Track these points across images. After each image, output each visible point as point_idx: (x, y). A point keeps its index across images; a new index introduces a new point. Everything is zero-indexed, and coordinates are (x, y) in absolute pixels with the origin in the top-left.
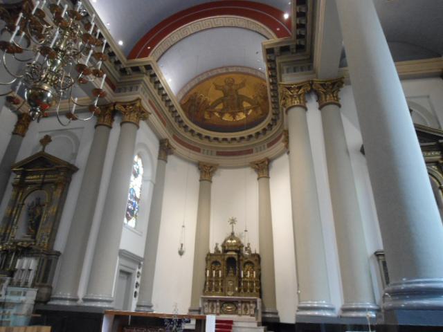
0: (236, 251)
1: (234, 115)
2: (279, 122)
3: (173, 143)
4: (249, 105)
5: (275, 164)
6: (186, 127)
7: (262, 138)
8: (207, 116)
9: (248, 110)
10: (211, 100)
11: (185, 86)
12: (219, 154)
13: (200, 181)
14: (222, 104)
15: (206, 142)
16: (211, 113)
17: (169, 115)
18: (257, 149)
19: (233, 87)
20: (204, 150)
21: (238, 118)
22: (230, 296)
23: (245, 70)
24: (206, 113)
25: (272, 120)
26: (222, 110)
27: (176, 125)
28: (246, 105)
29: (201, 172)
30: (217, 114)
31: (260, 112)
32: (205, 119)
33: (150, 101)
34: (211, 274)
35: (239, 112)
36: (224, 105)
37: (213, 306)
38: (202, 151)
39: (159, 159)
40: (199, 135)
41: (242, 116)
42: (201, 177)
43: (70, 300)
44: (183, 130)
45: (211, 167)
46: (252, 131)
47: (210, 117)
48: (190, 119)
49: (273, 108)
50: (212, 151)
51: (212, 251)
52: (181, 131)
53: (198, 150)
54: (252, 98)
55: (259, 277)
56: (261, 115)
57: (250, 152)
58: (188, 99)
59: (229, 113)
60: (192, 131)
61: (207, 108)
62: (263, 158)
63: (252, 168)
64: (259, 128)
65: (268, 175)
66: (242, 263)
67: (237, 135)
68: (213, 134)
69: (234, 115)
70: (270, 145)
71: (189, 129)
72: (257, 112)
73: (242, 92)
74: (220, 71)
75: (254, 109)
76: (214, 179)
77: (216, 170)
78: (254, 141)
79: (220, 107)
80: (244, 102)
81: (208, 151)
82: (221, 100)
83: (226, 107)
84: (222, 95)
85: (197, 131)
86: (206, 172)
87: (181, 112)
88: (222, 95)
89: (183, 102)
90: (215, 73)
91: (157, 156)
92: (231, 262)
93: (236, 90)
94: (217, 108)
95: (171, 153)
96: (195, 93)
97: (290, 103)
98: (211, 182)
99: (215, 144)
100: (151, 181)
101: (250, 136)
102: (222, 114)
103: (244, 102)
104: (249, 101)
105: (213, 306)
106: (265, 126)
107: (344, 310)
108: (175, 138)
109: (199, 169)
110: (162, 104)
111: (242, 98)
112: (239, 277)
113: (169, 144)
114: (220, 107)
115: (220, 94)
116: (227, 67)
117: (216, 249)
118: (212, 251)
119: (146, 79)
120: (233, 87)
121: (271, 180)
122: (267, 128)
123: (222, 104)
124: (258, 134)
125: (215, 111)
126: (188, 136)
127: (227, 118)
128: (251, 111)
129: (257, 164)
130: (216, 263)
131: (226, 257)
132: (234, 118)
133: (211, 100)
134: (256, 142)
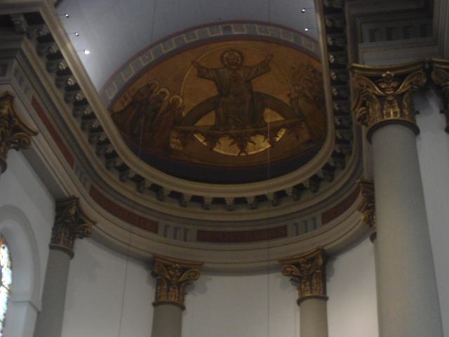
1: (242, 141)
2: (350, 160)
3: (91, 209)
4: (279, 118)
5: (342, 264)
6: (123, 169)
7: (309, 200)
8: (175, 143)
9: (275, 131)
10: (187, 103)
11: (124, 67)
12: (203, 237)
13: (155, 305)
14: (213, 113)
15: (171, 208)
16: (187, 137)
17: (82, 138)
18: (296, 225)
19: (241, 73)
20: (167, 227)
23: (270, 32)
24: (174, 134)
25: (335, 155)
26: (212, 128)
27: (98, 164)
28: (271, 117)
29: (159, 284)
31: (305, 136)
33: (34, 103)
35: (254, 134)
36: (218, 116)
38: (161, 229)
39: (51, 247)
40: (156, 189)
41: (261, 144)
42: (157, 297)
44: (115, 176)
45: (183, 270)
46: (286, 182)
47: (184, 145)
48: (135, 151)
49: (337, 127)
50: (186, 231)
52: (112, 179)
53: (151, 227)
54: (287, 101)
57: (280, 233)
58: (130, 99)
59: (231, 137)
60: (138, 180)
62: (312, 249)
63: (285, 273)
64: (302, 175)
65: (325, 292)
67: (249, 191)
68: (190, 188)
69: (242, 141)
70: (329, 217)
71: (132, 175)
72: (298, 137)
73: (264, 85)
74: (209, 33)
75: (291, 128)
76: (190, 300)
77: (196, 276)
78: (289, 207)
79: (208, 120)
80: (267, 111)
81: (176, 229)
84: (214, 92)
85: (150, 180)
86: (169, 284)
87: (111, 131)
88: (214, 92)
89: (118, 107)
90: (197, 35)
91: (49, 241)
93: (248, 82)
94: (200, 123)
95: (85, 234)
96: (149, 86)
97: (378, 114)
98: (183, 308)
99: (196, 213)
100: (31, 303)
101: (281, 195)
102: (212, 138)
103: (267, 111)
104: (279, 108)
106: (318, 170)
108: (98, 197)
109: (154, 275)
110: (66, 111)
111: (262, 101)
113: (80, 211)
114: (208, 120)
115: (208, 89)
116: (226, 24)
120: (241, 73)
121: (330, 305)
122: (321, 175)
123: (213, 113)
124: (299, 189)
125: (196, 132)
126: (128, 191)
127: (225, 148)
129: (298, 265)
132: (243, 148)
133: (187, 103)
134: (294, 209)
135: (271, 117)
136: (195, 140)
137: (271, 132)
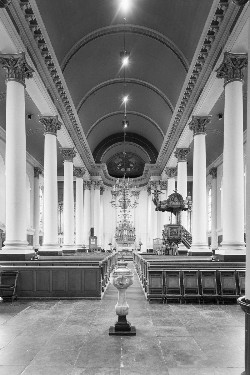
1: (126, 169)
8: (114, 169)
16: (116, 168)
21: (127, 170)
30: (118, 168)
32: (113, 171)
41: (129, 170)
56: (138, 171)
61: (115, 166)
69: (126, 169)
75: (135, 168)
79: (120, 165)
94: (119, 165)
102: (120, 168)
104: (133, 164)
111: (131, 162)
114: (120, 165)
125: (118, 167)
127: (122, 170)
135: (131, 165)
136: (117, 168)
137: (131, 168)
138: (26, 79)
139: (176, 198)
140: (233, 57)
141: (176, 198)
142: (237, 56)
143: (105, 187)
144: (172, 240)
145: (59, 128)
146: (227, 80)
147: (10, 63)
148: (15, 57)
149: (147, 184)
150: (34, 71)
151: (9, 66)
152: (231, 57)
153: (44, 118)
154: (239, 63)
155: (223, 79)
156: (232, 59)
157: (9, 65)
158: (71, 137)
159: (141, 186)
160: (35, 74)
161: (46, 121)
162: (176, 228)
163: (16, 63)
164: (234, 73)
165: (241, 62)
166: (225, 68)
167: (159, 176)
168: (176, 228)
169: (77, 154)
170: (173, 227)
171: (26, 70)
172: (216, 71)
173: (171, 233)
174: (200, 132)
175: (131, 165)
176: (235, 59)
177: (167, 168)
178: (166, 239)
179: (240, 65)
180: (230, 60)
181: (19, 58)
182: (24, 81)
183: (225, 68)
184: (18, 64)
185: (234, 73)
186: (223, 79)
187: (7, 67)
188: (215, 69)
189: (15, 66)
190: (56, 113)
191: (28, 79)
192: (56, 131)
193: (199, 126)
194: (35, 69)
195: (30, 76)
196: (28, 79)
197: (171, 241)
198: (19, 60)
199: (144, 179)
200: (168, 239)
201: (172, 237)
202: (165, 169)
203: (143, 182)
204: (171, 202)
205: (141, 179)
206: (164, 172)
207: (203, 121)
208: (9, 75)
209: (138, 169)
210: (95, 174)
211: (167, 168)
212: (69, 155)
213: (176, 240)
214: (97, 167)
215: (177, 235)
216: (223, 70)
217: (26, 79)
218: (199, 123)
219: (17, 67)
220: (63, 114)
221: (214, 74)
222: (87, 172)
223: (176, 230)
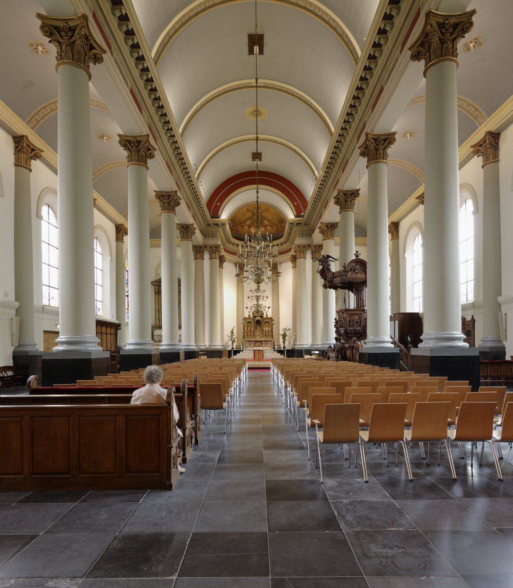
0: (260, 317)
4: (268, 223)
8: (240, 229)
9: (267, 226)
16: (243, 227)
22: (258, 339)
26: (250, 224)
28: (266, 222)
34: (248, 329)
37: (250, 343)
43: (185, 346)
51: (247, 317)
55: (272, 329)
66: (263, 323)
79: (249, 222)
82: (250, 218)
83: (252, 222)
92: (258, 322)
102: (249, 227)
105: (250, 343)
107: (312, 345)
111: (265, 218)
112: (263, 330)
114: (249, 222)
115: (250, 214)
117: (249, 316)
118: (247, 317)
119: (221, 230)
128: (268, 227)
130: (249, 322)
131: (256, 320)
138: (91, 65)
139: (358, 267)
140: (441, 21)
141: (358, 267)
142: (447, 19)
143: (227, 256)
144: (351, 333)
145: (152, 156)
146: (431, 62)
147: (63, 34)
148: (72, 24)
149: (289, 250)
150: (105, 52)
151: (61, 40)
152: (437, 20)
153: (127, 139)
154: (452, 31)
155: (423, 62)
156: (439, 24)
157: (62, 37)
158: (172, 174)
159: (281, 253)
160: (106, 57)
161: (130, 144)
162: (357, 314)
163: (73, 35)
164: (442, 49)
165: (455, 29)
166: (426, 41)
167: (310, 237)
168: (357, 314)
169: (182, 202)
170: (352, 312)
171: (92, 48)
172: (409, 49)
173: (350, 322)
174: (379, 159)
175: (266, 222)
176: (445, 23)
177: (321, 223)
178: (342, 332)
179: (452, 34)
180: (434, 24)
181: (77, 26)
182: (88, 67)
183: (426, 41)
184: (76, 36)
185: (442, 49)
186: (423, 62)
187: (59, 42)
188: (409, 44)
189: (72, 40)
190: (146, 131)
191: (95, 64)
192: (146, 160)
193: (377, 150)
194: (105, 47)
195: (98, 59)
196: (95, 64)
197: (349, 335)
198: (78, 29)
199: (286, 243)
200: (346, 333)
201: (352, 328)
202: (319, 225)
203: (285, 247)
204: (350, 273)
205: (282, 244)
206: (317, 230)
207: (382, 142)
208: (61, 55)
209: (276, 228)
210: (211, 235)
211: (321, 223)
212: (169, 203)
213: (358, 333)
214: (214, 224)
215: (360, 326)
216: (422, 45)
217: (91, 65)
218: (377, 144)
219: (75, 42)
220: (157, 135)
221: (407, 53)
222: (197, 232)
223: (357, 317)
